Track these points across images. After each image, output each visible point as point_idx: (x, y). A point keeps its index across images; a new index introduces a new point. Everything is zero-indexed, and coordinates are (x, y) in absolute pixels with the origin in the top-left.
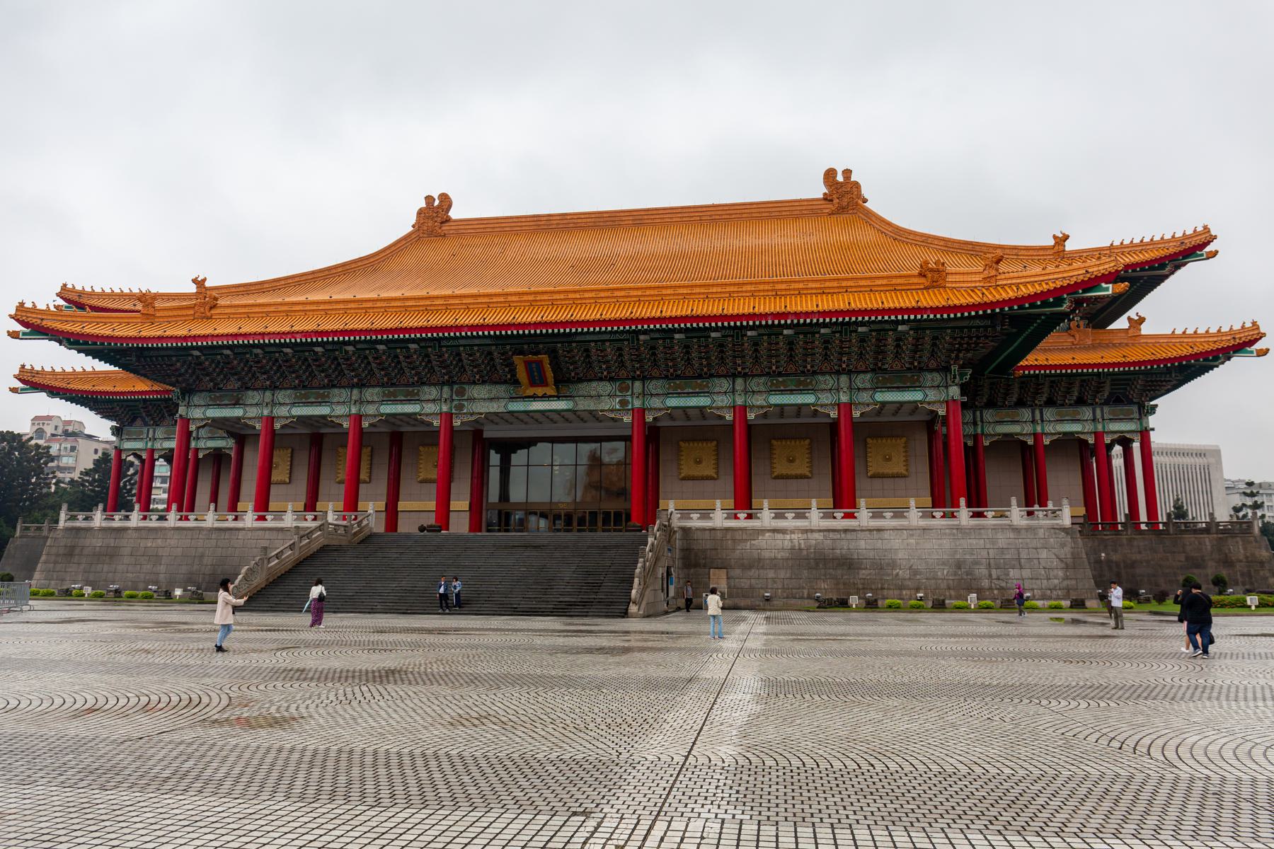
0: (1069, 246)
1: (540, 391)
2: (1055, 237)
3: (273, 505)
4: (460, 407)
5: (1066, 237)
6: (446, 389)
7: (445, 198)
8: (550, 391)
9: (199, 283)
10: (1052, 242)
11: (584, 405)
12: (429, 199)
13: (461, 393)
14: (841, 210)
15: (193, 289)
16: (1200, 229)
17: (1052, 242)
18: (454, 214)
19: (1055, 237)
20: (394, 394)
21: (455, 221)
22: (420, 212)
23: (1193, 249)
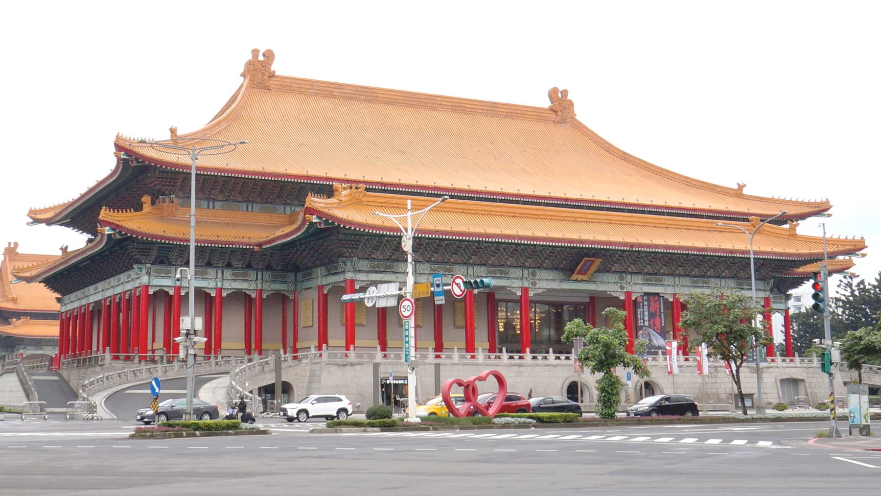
0: (745, 191)
1: (580, 277)
2: (738, 184)
3: (446, 344)
4: (534, 284)
5: (745, 186)
6: (526, 272)
7: (269, 55)
8: (585, 278)
9: (173, 131)
10: (736, 187)
11: (601, 288)
12: (255, 52)
13: (534, 274)
14: (563, 121)
15: (167, 136)
16: (824, 200)
17: (736, 187)
18: (279, 68)
19: (738, 184)
20: (494, 272)
21: (279, 77)
22: (249, 64)
23: (821, 210)
